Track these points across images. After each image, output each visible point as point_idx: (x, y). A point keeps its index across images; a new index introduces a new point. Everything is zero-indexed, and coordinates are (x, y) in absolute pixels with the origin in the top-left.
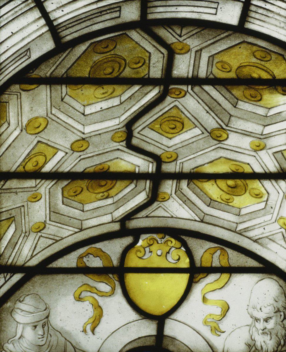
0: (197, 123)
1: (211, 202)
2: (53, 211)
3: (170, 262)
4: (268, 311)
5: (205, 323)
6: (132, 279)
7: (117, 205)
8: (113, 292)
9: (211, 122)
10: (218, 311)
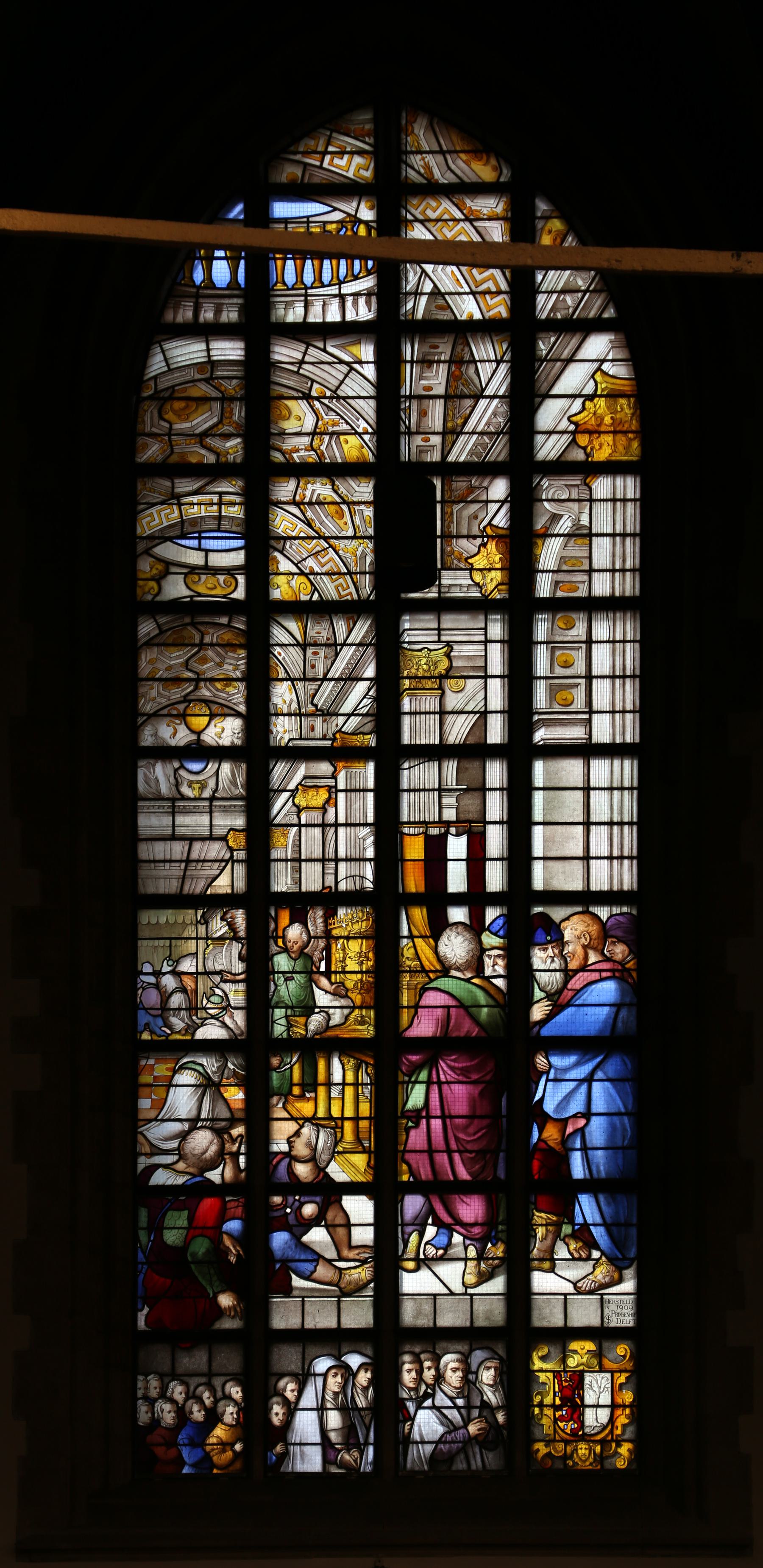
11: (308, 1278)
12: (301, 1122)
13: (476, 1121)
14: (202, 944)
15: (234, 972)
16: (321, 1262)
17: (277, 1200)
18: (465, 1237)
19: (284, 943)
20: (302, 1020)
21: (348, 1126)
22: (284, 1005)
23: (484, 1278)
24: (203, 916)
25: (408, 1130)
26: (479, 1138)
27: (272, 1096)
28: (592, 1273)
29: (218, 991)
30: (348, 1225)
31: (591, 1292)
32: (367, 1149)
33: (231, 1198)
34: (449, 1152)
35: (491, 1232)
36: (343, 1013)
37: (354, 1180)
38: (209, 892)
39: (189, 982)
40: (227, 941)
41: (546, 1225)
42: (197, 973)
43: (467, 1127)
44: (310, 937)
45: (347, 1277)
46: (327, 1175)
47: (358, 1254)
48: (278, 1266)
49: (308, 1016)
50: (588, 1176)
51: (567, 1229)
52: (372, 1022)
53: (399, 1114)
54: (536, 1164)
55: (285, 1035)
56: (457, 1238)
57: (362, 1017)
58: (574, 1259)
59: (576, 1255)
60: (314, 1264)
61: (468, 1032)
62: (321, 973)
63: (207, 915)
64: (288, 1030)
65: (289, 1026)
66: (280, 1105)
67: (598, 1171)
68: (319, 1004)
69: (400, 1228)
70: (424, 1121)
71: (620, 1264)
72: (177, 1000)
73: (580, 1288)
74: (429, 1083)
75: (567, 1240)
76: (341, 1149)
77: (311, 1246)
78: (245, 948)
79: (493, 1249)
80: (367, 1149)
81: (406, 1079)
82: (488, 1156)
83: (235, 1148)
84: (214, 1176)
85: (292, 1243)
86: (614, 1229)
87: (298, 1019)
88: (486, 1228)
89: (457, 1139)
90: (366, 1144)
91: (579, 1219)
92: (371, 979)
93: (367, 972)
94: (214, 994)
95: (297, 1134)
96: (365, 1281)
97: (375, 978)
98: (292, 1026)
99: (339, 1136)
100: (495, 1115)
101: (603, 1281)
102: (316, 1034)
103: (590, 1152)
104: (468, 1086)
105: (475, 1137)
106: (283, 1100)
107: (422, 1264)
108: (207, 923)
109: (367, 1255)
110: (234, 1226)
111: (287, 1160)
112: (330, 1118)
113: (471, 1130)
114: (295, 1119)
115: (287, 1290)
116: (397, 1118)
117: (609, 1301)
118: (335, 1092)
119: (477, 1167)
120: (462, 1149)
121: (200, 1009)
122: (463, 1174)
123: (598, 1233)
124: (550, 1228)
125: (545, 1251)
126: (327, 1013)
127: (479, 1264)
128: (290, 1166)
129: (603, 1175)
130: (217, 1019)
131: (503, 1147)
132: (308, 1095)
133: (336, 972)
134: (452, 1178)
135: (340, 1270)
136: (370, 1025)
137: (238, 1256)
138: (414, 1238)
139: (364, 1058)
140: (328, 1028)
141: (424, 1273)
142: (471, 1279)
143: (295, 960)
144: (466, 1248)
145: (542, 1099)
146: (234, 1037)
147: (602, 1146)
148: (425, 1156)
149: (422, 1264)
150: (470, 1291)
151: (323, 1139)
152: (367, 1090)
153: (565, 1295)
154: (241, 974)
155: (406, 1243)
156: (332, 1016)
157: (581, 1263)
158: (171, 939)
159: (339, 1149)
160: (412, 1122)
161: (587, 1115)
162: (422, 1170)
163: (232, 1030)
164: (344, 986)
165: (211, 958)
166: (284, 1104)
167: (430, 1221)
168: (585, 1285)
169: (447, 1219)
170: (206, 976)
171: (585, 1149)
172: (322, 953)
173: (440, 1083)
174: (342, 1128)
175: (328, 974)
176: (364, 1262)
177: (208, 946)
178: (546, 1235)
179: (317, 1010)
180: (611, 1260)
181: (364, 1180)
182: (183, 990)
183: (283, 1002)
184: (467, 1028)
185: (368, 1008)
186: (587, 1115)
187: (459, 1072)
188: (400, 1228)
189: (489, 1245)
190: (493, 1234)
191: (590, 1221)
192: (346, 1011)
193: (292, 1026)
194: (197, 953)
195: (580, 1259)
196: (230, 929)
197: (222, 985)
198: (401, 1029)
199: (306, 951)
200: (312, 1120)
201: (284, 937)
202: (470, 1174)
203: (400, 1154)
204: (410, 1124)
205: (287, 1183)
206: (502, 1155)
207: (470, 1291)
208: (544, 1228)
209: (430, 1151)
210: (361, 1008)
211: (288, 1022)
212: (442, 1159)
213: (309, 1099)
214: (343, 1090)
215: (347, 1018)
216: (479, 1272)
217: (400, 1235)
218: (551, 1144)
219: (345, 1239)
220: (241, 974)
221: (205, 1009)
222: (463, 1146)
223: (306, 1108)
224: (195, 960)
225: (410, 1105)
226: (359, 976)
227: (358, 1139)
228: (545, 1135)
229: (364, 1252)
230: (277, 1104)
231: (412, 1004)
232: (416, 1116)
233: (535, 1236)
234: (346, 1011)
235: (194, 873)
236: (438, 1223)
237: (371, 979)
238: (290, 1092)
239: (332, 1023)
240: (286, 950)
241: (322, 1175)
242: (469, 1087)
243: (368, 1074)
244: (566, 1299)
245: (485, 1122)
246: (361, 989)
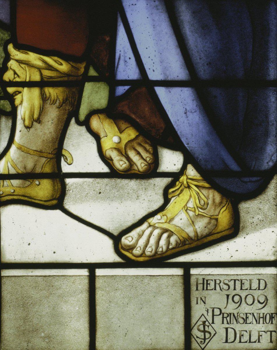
41: (42, 84)
73: (130, 248)
101: (190, 231)
117: (205, 283)
153: (92, 267)
157: (133, 184)
178: (42, 110)
208: (36, 91)
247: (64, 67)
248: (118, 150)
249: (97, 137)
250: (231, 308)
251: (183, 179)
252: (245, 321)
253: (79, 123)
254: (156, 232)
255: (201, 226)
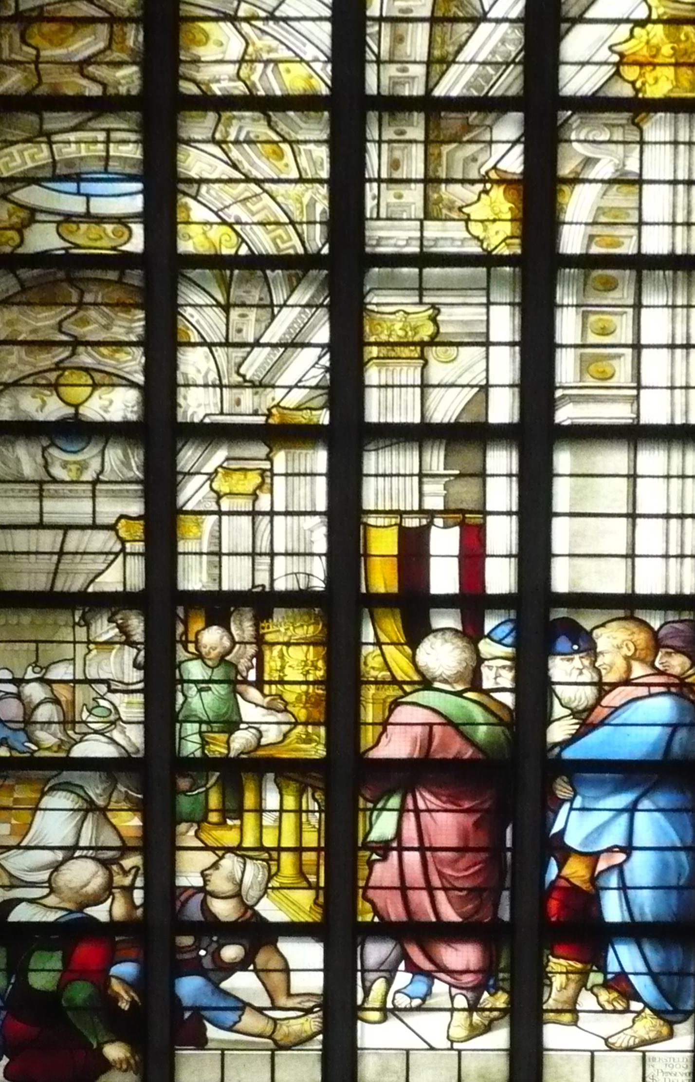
0: (97, 322)
1: (103, 356)
2: (20, 360)
3: (82, 381)
4: (134, 402)
5: (101, 408)
6: (62, 390)
7: (53, 357)
8: (52, 395)
9: (104, 322)
10: (107, 403)
11: (230, 1029)
12: (220, 853)
13: (469, 856)
14: (81, 649)
15: (126, 681)
16: (248, 1009)
17: (187, 941)
18: (451, 985)
19: (197, 649)
20: (223, 737)
21: (287, 859)
22: (197, 719)
23: (476, 1032)
24: (83, 617)
25: (371, 864)
26: (473, 874)
27: (179, 824)
28: (631, 1027)
29: (102, 702)
30: (286, 970)
31: (629, 1049)
32: (314, 885)
33: (121, 938)
34: (430, 889)
35: (488, 980)
36: (280, 731)
37: (295, 920)
38: (90, 590)
39: (63, 692)
40: (118, 646)
42: (75, 681)
43: (456, 861)
44: (234, 643)
45: (285, 1028)
46: (256, 914)
47: (300, 1003)
48: (187, 1015)
49: (231, 733)
50: (627, 919)
51: (596, 978)
52: (323, 741)
53: (360, 844)
54: (553, 905)
55: (198, 754)
56: (440, 988)
57: (307, 734)
58: (604, 1011)
59: (609, 1007)
60: (239, 1013)
61: (459, 752)
62: (250, 684)
63: (88, 616)
64: (203, 747)
65: (204, 743)
66: (192, 833)
67: (642, 914)
68: (245, 719)
69: (359, 974)
70: (395, 854)
71: (669, 1017)
72: (45, 712)
73: (613, 1044)
74: (402, 811)
75: (595, 990)
76: (277, 885)
77: (234, 993)
78: (142, 653)
79: (491, 999)
80: (314, 885)
81: (370, 805)
82: (485, 895)
83: (127, 881)
84: (100, 913)
85: (209, 989)
86: (664, 979)
87: (216, 735)
88: (480, 976)
89: (441, 875)
90: (312, 879)
91: (613, 966)
92: (320, 692)
93: (314, 683)
94: (99, 706)
95: (215, 866)
96: (309, 1033)
97: (327, 690)
98: (208, 743)
99: (274, 869)
100: (496, 848)
101: (647, 1037)
102: (242, 753)
103: (631, 893)
104: (456, 815)
105: (466, 873)
106: (195, 827)
107: (389, 1014)
108: (88, 625)
109: (312, 1004)
110: (126, 969)
111: (200, 896)
112: (261, 848)
113: (461, 865)
114: (213, 849)
115: (201, 1042)
116: (356, 849)
117: (654, 1059)
118: (268, 820)
119: (470, 906)
120: (448, 886)
121: (79, 722)
122: (450, 914)
123: (643, 985)
124: (571, 976)
125: (565, 1002)
126: (258, 729)
127: (471, 1016)
128: (204, 903)
129: (649, 918)
130: (103, 734)
131: (508, 883)
132: (229, 822)
133: (270, 683)
134: (434, 919)
135: (275, 1021)
136: (318, 743)
137: (133, 1003)
138: (379, 987)
139: (310, 781)
140: (259, 746)
141: (393, 1022)
142: (459, 1030)
143: (213, 668)
144: (452, 998)
145: (562, 832)
146: (126, 755)
147: (650, 885)
148: (398, 892)
149: (389, 1014)
150: (456, 1046)
151: (253, 873)
152: (314, 819)
153: (592, 1052)
154: (138, 683)
155: (367, 992)
156: (264, 734)
157: (615, 1016)
158: (37, 642)
159: (274, 883)
160: (377, 854)
161: (628, 849)
162: (390, 910)
163: (123, 748)
164: (282, 699)
165: (94, 665)
166: (196, 832)
167: (402, 966)
168: (621, 1041)
169: (427, 965)
170: (87, 686)
171: (623, 888)
172: (251, 661)
173: (417, 812)
174: (278, 860)
175: (259, 684)
176: (308, 1011)
177: (90, 651)
178: (567, 985)
179: (242, 726)
180: (658, 1013)
181: (310, 920)
182: (56, 701)
183: (196, 716)
184: (457, 748)
185: (316, 724)
186: (628, 849)
187: (444, 799)
188: (359, 974)
189: (486, 995)
190: (491, 982)
191: (628, 969)
192: (285, 728)
193: (208, 743)
194: (74, 659)
195: (615, 1011)
196: (121, 631)
197: (110, 696)
198: (362, 750)
199: (228, 658)
200: (237, 850)
201: (196, 642)
202: (459, 915)
203: (360, 891)
204: (375, 857)
205: (200, 922)
206: (506, 894)
207: (456, 1046)
208: (564, 976)
209: (404, 888)
210: (306, 724)
211: (202, 738)
212: (420, 899)
213: (231, 827)
214: (280, 818)
215: (286, 736)
216: (471, 1025)
217: (359, 982)
218: (577, 882)
219: (282, 986)
220: (138, 683)
221: (85, 723)
222: (450, 883)
223: (229, 838)
224: (71, 667)
225: (374, 836)
226: (304, 688)
227: (301, 874)
228: (567, 871)
229: (309, 1001)
230: (187, 832)
231: (379, 719)
232: (384, 848)
233: (551, 985)
234: (285, 728)
235: (67, 567)
236: (413, 969)
237: (320, 692)
238: (205, 819)
239: (264, 741)
240: (199, 656)
241: (249, 913)
242: (461, 817)
243: (315, 800)
244: (592, 1057)
245: (483, 855)
246: (307, 702)
247: (579, 966)
248: (608, 1002)
249: (597, 996)
250: (668, 1070)
251: (643, 1014)
252: (675, 1075)
253: (586, 989)
254: (628, 1037)
255: (652, 1035)
